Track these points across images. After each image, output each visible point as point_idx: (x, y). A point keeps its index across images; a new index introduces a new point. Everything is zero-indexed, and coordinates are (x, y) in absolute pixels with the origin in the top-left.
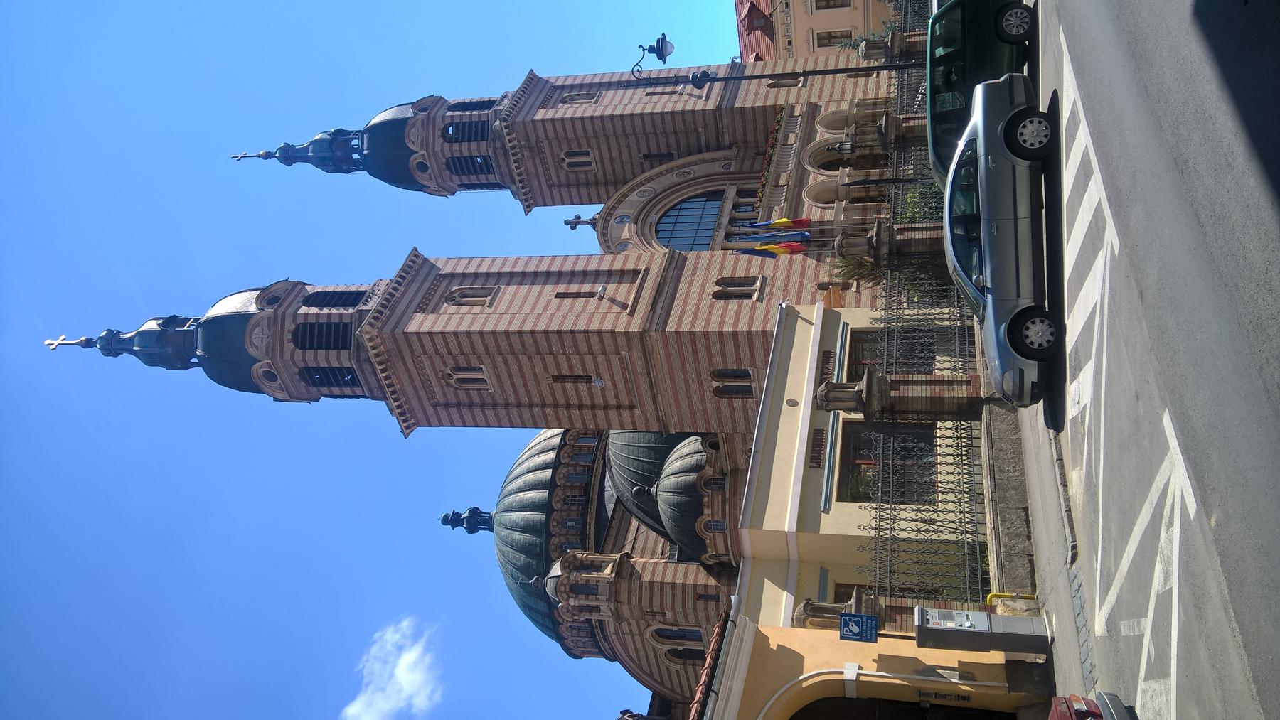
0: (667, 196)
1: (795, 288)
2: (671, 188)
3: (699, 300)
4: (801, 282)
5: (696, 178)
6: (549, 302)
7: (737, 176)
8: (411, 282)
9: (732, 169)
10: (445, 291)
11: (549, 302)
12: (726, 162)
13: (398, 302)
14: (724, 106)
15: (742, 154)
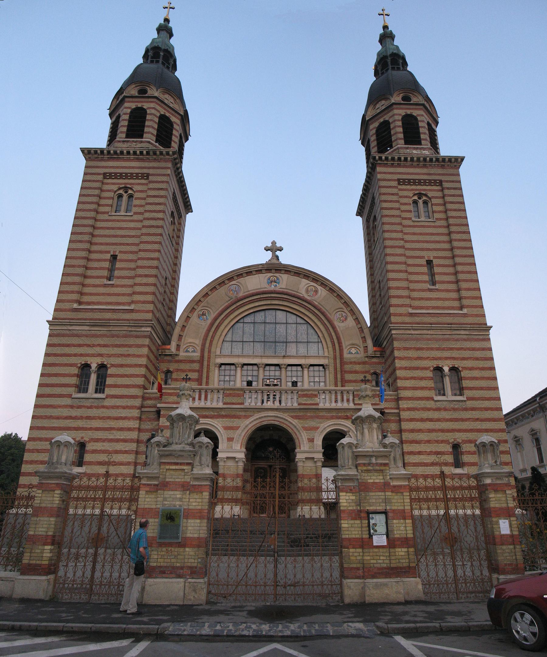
0: (309, 310)
1: (82, 425)
2: (319, 310)
3: (81, 355)
4: (91, 429)
5: (334, 328)
6: (108, 252)
7: (338, 361)
8: (142, 160)
9: (346, 355)
10: (131, 184)
11: (108, 252)
12: (362, 349)
13: (118, 159)
14: (393, 332)
15: (374, 360)
